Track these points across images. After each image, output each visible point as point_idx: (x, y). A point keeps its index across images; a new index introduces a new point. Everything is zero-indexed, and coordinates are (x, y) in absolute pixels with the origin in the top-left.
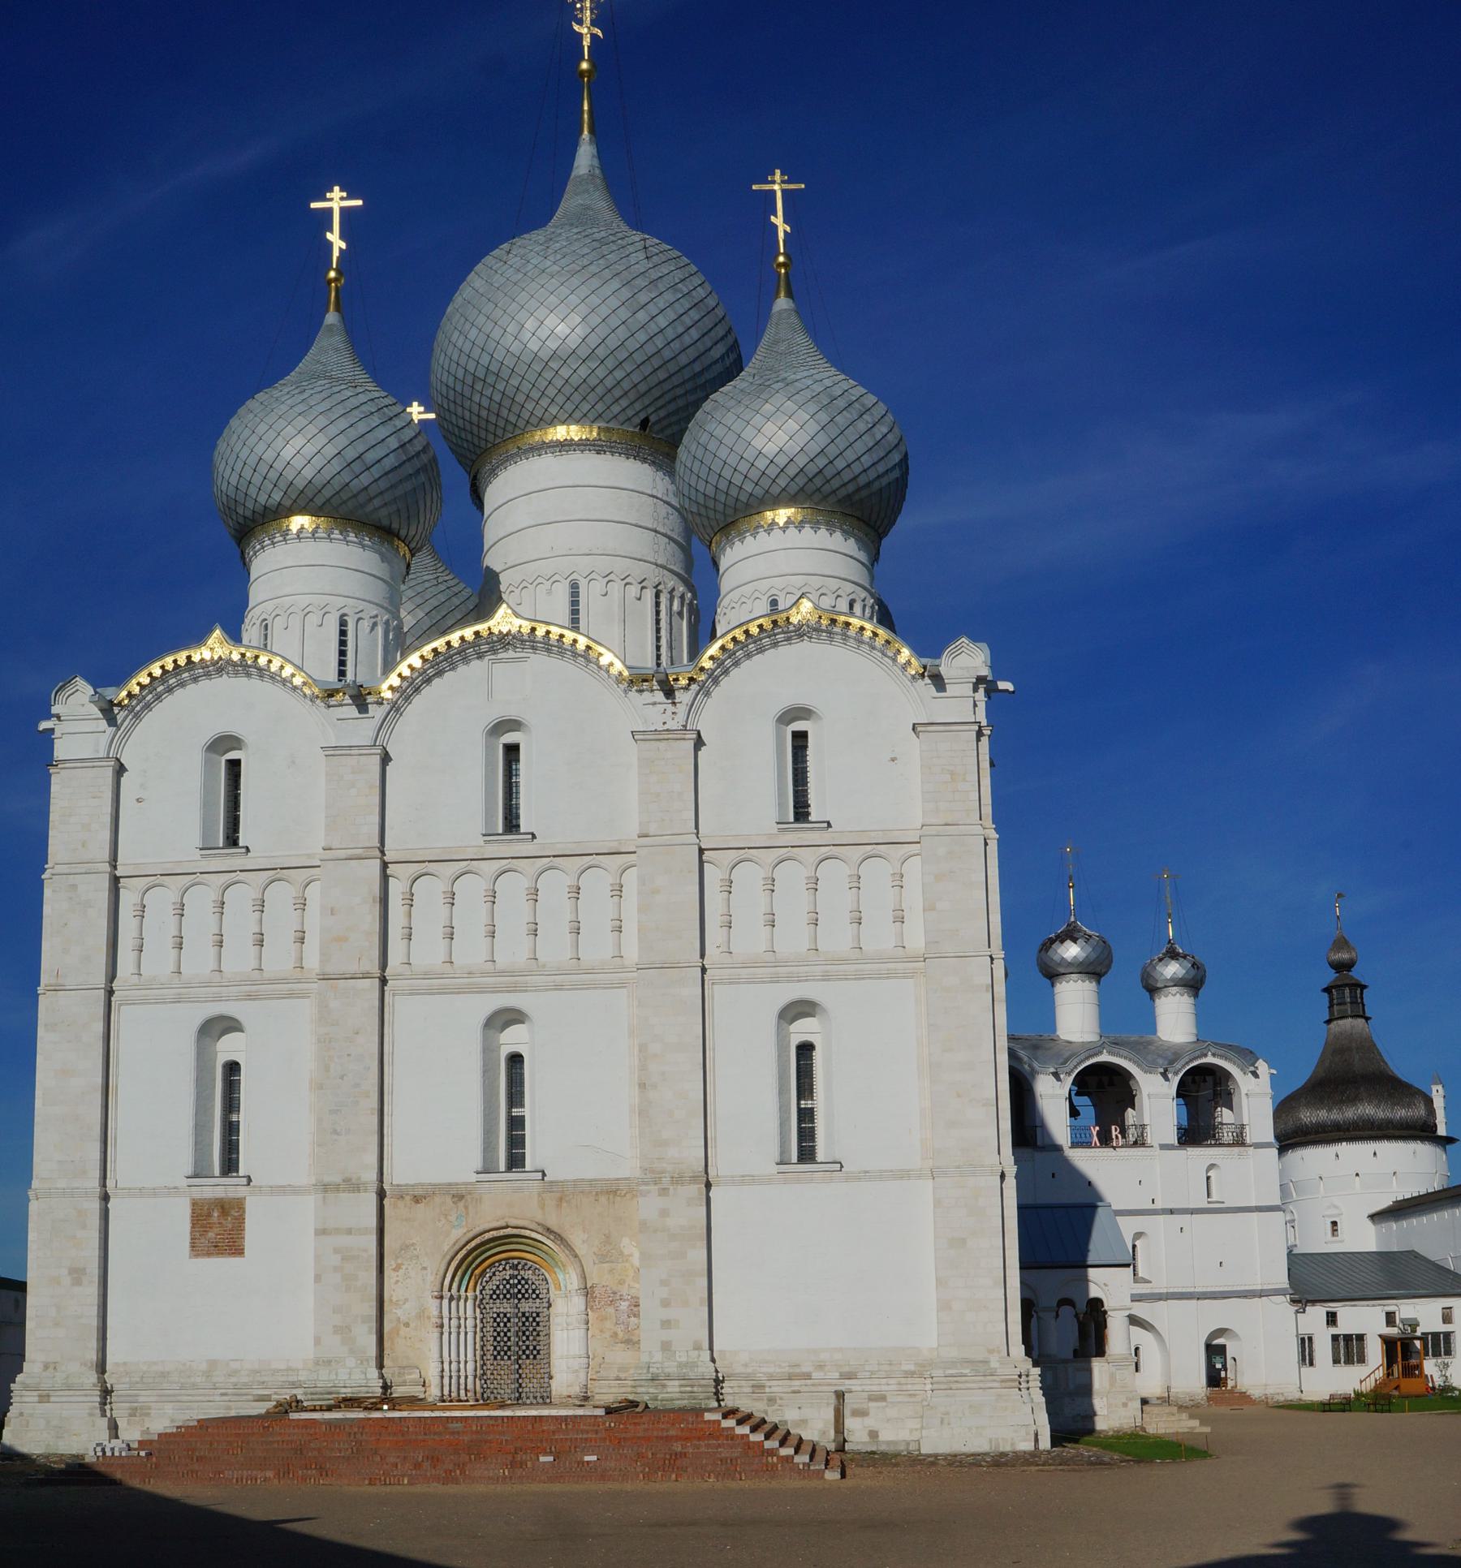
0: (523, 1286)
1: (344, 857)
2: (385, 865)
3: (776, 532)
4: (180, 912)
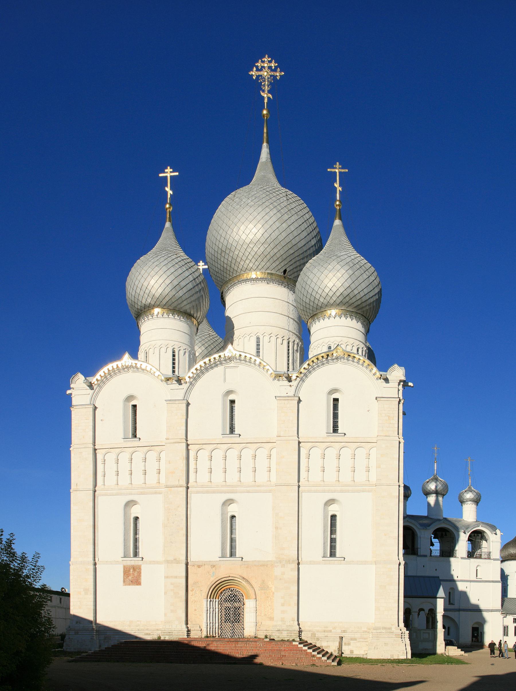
0: (235, 597)
1: (173, 442)
2: (188, 445)
3: (332, 319)
4: (117, 462)
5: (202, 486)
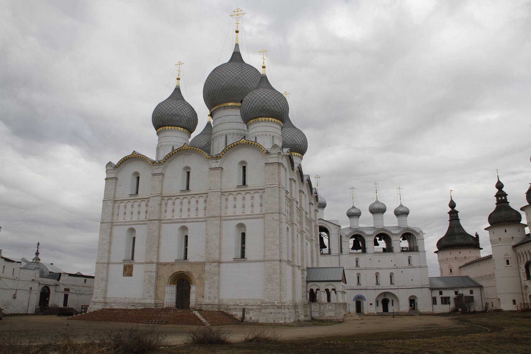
5: (168, 220)
